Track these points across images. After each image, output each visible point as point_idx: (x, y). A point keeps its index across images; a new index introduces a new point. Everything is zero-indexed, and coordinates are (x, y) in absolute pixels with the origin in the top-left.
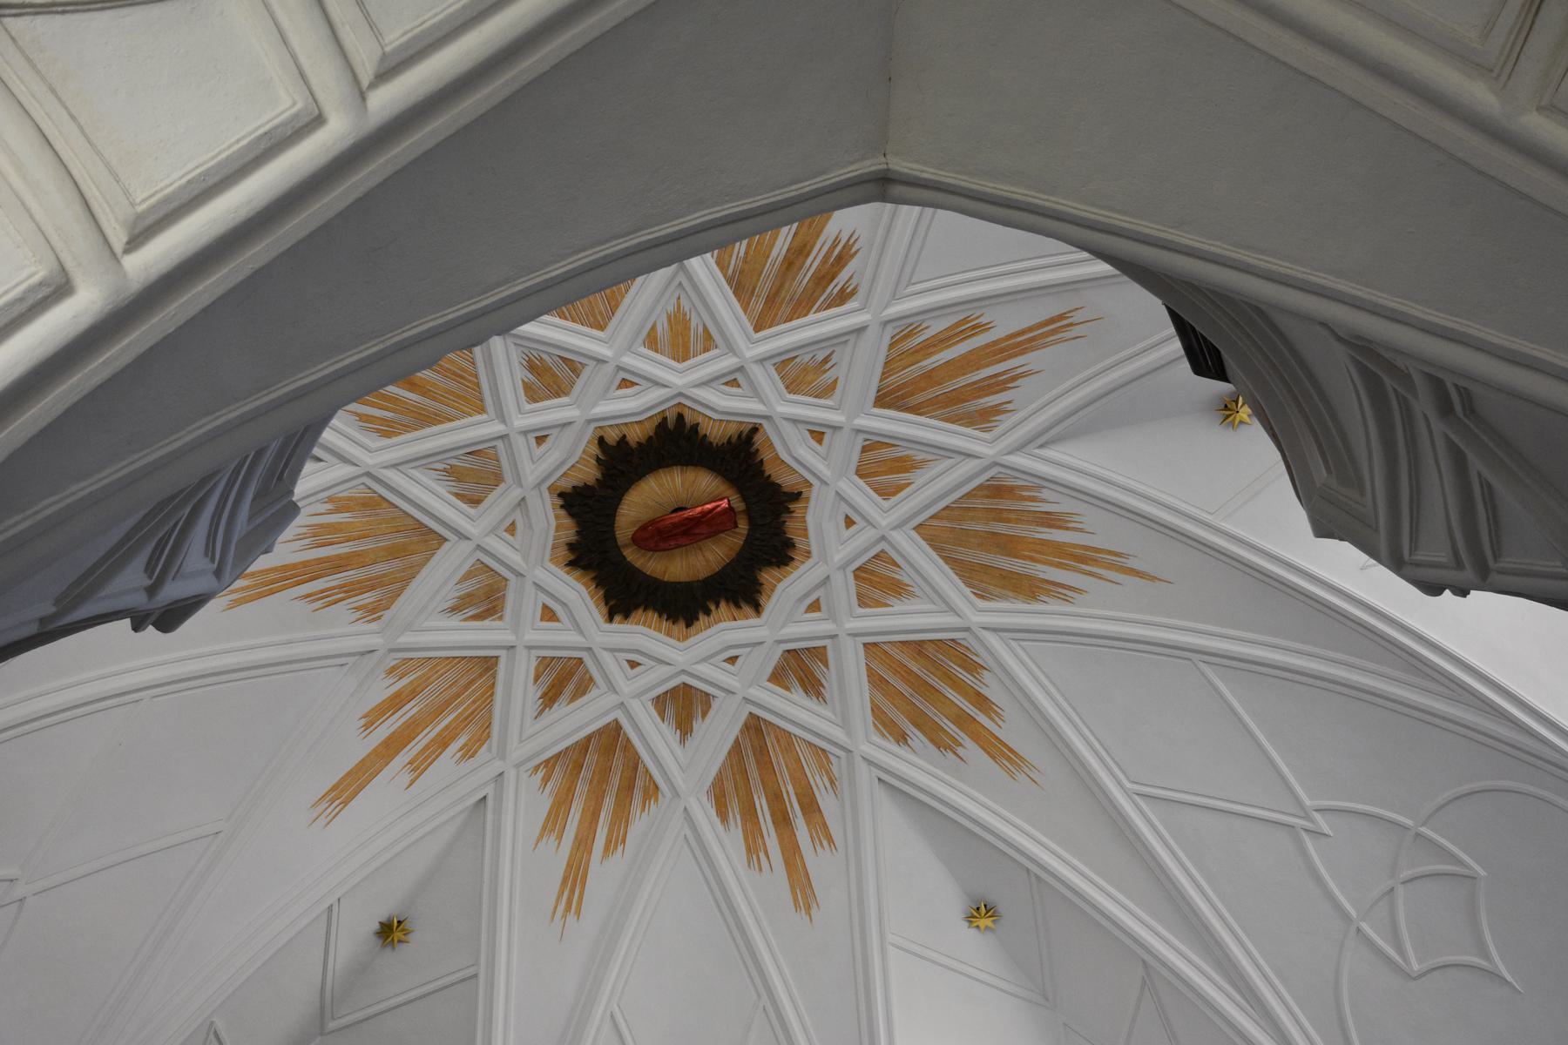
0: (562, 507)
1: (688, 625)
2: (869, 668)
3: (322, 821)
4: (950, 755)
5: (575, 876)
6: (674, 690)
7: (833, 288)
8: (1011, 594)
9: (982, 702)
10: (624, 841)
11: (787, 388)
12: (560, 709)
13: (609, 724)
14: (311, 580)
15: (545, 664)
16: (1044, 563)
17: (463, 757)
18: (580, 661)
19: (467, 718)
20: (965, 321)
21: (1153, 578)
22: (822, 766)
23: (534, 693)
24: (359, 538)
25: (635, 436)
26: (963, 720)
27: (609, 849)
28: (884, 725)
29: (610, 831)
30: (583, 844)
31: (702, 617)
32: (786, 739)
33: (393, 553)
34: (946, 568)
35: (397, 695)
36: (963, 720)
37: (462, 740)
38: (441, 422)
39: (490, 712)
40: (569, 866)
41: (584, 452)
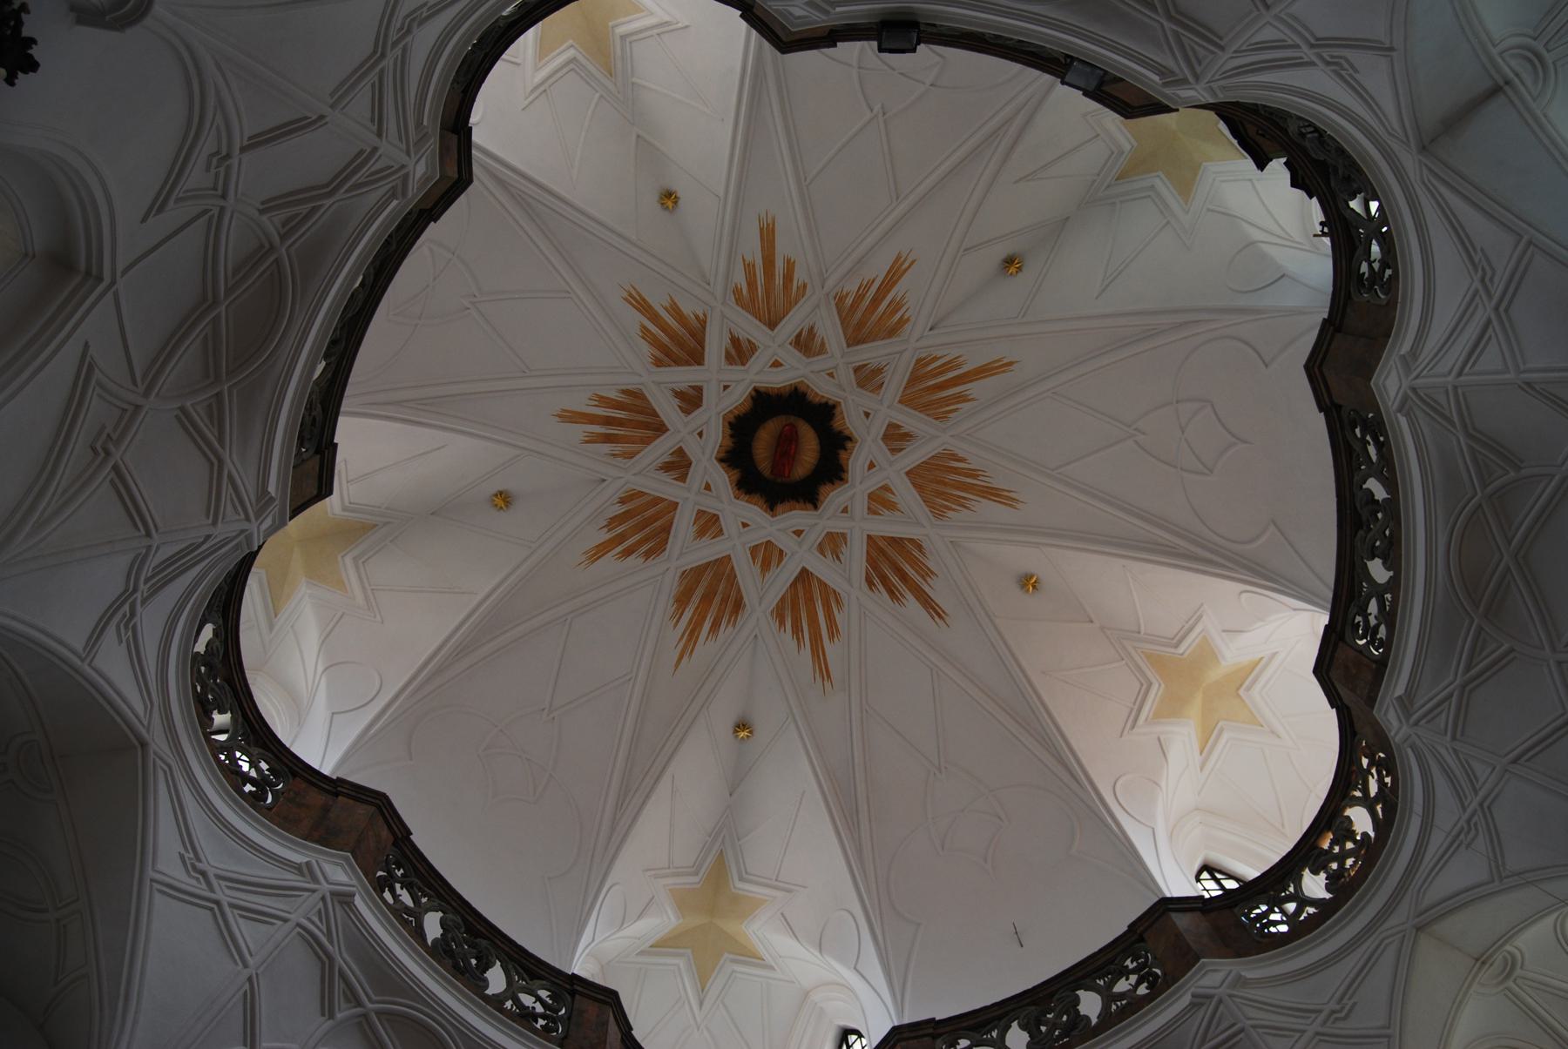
0: (827, 403)
1: (730, 423)
2: (663, 500)
3: (763, 215)
4: (605, 523)
5: (643, 306)
6: (700, 399)
7: (876, 581)
8: (682, 589)
9: (628, 552)
10: (643, 338)
11: (831, 533)
12: (726, 341)
13: (703, 359)
14: (879, 288)
15: (753, 348)
16: (694, 613)
17: (736, 287)
18: (743, 364)
19: (754, 300)
20: (838, 631)
21: (677, 665)
22: (625, 453)
23: (742, 336)
24: (881, 317)
25: (843, 455)
26: (621, 538)
27: (644, 328)
28: (633, 495)
29: (652, 334)
30: (654, 317)
31: (729, 432)
32: (647, 441)
33: (861, 324)
34: (705, 561)
35: (791, 280)
36: (621, 538)
37: (745, 291)
38: (908, 383)
39: (748, 311)
40: (650, 306)
41: (848, 428)
